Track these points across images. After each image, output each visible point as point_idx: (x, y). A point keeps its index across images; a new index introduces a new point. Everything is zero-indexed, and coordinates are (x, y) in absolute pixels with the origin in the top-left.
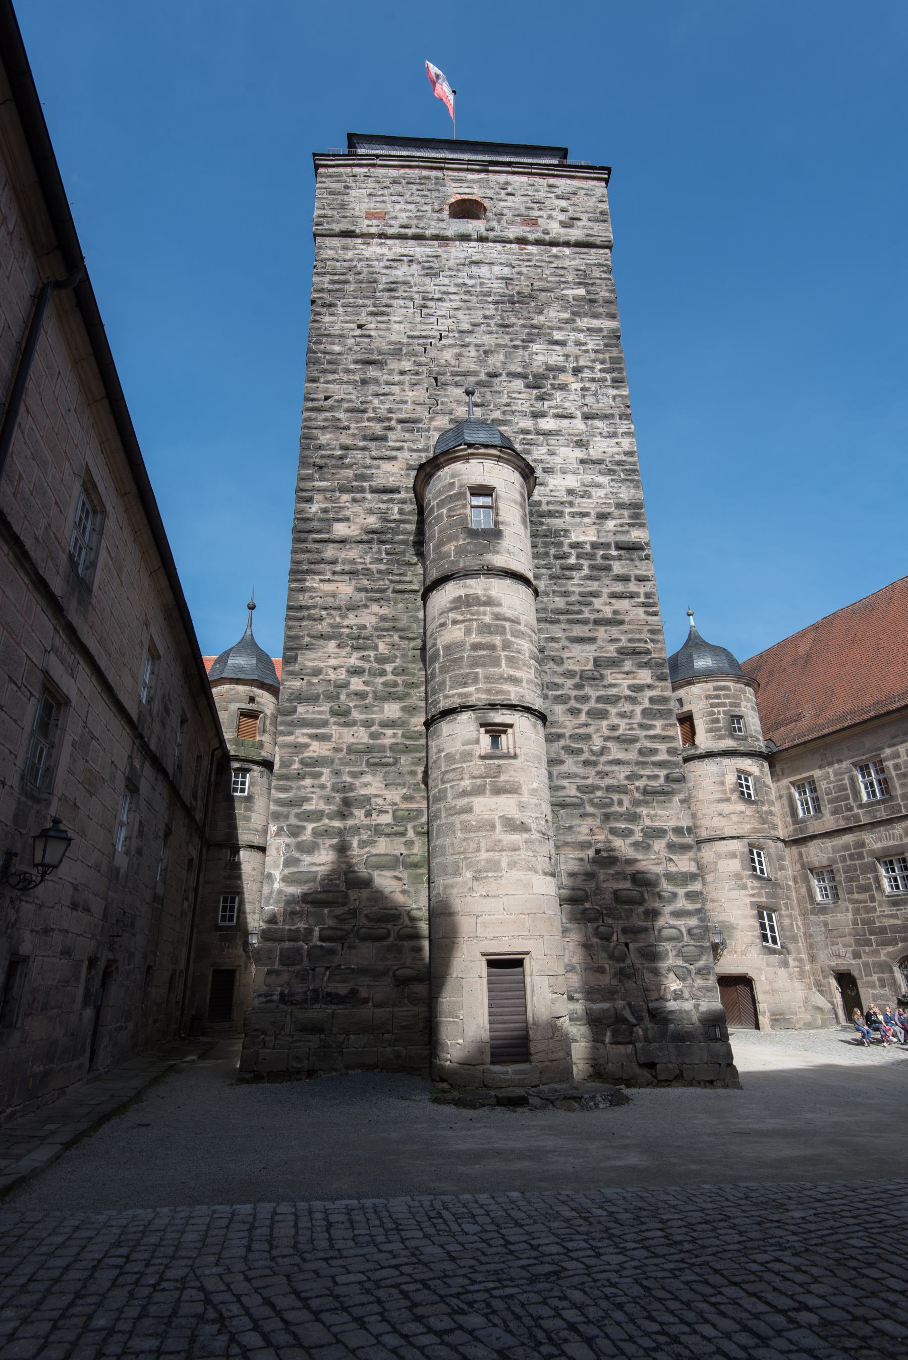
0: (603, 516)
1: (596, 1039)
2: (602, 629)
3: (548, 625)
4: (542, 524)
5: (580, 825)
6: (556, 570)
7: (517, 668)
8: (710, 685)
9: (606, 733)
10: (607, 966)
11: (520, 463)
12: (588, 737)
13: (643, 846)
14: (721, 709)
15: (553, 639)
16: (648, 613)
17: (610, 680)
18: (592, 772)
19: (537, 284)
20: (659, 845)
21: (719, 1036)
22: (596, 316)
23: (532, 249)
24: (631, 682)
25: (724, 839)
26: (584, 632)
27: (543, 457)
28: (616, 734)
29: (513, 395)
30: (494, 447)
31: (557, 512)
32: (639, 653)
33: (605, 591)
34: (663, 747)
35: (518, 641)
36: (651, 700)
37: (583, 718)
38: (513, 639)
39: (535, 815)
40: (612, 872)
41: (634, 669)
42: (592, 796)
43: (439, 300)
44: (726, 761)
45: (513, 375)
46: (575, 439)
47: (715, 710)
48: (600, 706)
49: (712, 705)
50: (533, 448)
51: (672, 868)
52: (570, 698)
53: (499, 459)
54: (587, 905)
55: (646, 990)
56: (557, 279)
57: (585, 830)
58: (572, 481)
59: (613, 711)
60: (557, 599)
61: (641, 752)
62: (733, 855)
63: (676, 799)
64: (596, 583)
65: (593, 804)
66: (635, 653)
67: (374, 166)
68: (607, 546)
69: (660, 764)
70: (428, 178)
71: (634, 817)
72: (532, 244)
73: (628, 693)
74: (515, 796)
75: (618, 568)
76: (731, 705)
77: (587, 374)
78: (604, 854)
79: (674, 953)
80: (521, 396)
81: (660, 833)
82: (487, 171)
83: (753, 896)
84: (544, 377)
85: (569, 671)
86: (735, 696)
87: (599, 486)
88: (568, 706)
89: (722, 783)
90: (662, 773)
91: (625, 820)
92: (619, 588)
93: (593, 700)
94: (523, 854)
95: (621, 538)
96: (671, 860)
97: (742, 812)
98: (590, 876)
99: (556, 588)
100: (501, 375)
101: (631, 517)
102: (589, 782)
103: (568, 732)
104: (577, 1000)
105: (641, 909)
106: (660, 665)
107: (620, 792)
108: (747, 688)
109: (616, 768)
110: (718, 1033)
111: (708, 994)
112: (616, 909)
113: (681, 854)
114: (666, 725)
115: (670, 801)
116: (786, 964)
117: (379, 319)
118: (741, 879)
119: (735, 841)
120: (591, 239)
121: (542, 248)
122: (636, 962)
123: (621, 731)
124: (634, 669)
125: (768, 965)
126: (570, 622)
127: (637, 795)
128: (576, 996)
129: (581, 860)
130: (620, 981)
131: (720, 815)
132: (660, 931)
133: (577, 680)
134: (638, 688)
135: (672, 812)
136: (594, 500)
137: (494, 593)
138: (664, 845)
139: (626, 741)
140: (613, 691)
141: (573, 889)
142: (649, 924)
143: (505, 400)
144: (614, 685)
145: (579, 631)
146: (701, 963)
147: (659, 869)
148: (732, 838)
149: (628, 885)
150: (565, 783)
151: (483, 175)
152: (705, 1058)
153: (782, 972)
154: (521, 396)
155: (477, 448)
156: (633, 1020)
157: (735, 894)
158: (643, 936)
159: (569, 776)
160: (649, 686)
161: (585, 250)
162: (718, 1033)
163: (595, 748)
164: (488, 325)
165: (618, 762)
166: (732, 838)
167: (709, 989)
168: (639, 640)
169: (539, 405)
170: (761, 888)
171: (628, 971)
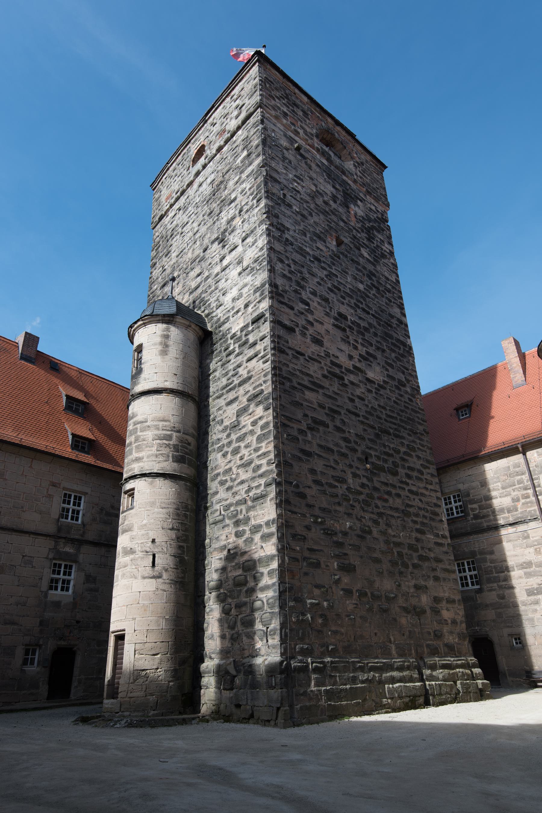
0: (246, 306)
1: (218, 687)
2: (241, 388)
3: (218, 400)
4: (220, 332)
5: (221, 535)
6: (224, 359)
7: (141, 451)
9: (239, 463)
10: (227, 634)
11: (158, 319)
12: (230, 469)
13: (250, 541)
15: (219, 409)
16: (264, 362)
17: (243, 423)
18: (230, 493)
19: (224, 171)
20: (257, 537)
21: (274, 685)
22: (250, 164)
23: (225, 149)
24: (252, 420)
26: (233, 395)
27: (223, 286)
28: (243, 461)
29: (212, 256)
30: (138, 320)
31: (226, 319)
32: (257, 395)
33: (245, 358)
34: (264, 461)
35: (144, 433)
36: (262, 428)
37: (229, 456)
38: (141, 434)
39: (140, 542)
40: (234, 564)
41: (255, 409)
42: (229, 511)
43: (187, 223)
45: (213, 242)
46: (237, 260)
48: (237, 445)
50: (220, 283)
51: (263, 554)
52: (224, 446)
53: (145, 324)
54: (222, 591)
55: (244, 650)
56: (233, 157)
57: (224, 537)
58: (234, 293)
59: (242, 444)
60: (224, 379)
61: (254, 471)
63: (269, 498)
64: (241, 356)
65: (229, 518)
66: (256, 396)
67: (168, 169)
68: (247, 326)
69: (261, 476)
70: (185, 153)
71: (247, 520)
72: (225, 145)
73: (251, 428)
74: (129, 533)
75: (251, 338)
77: (245, 208)
78: (232, 552)
79: (259, 619)
80: (216, 253)
81: (256, 529)
82: (207, 121)
84: (225, 230)
85: (225, 427)
87: (245, 285)
88: (223, 452)
90: (262, 481)
91: (243, 524)
92: (251, 352)
93: (234, 442)
94: (128, 569)
95: (255, 314)
96: (262, 547)
98: (224, 569)
99: (224, 372)
100: (208, 247)
101: (260, 296)
102: (228, 502)
103: (221, 470)
104: (213, 659)
105: (245, 589)
106: (267, 399)
107: (241, 504)
109: (240, 487)
110: (274, 682)
111: (274, 651)
112: (234, 591)
113: (269, 541)
114: (267, 444)
115: (266, 502)
117: (168, 256)
120: (249, 112)
121: (229, 143)
122: (240, 629)
123: (245, 459)
124: (255, 409)
126: (228, 392)
127: (250, 503)
128: (213, 656)
129: (221, 559)
130: (232, 644)
132: (253, 604)
133: (228, 431)
134: (254, 423)
135: (266, 510)
136: (245, 296)
137: (135, 410)
138: (259, 537)
139: (245, 465)
140: (244, 431)
141: (216, 581)
142: (248, 599)
143: (210, 261)
144: (244, 427)
145: (231, 396)
146: (272, 627)
147: (256, 556)
149: (240, 572)
150: (217, 507)
151: (205, 125)
152: (266, 702)
154: (216, 253)
155: (133, 326)
156: (234, 672)
158: (244, 609)
159: (220, 501)
160: (260, 418)
161: (248, 122)
162: (274, 682)
163: (234, 476)
164: (204, 220)
165: (242, 482)
167: (274, 647)
168: (258, 386)
169: (223, 252)
171: (235, 636)
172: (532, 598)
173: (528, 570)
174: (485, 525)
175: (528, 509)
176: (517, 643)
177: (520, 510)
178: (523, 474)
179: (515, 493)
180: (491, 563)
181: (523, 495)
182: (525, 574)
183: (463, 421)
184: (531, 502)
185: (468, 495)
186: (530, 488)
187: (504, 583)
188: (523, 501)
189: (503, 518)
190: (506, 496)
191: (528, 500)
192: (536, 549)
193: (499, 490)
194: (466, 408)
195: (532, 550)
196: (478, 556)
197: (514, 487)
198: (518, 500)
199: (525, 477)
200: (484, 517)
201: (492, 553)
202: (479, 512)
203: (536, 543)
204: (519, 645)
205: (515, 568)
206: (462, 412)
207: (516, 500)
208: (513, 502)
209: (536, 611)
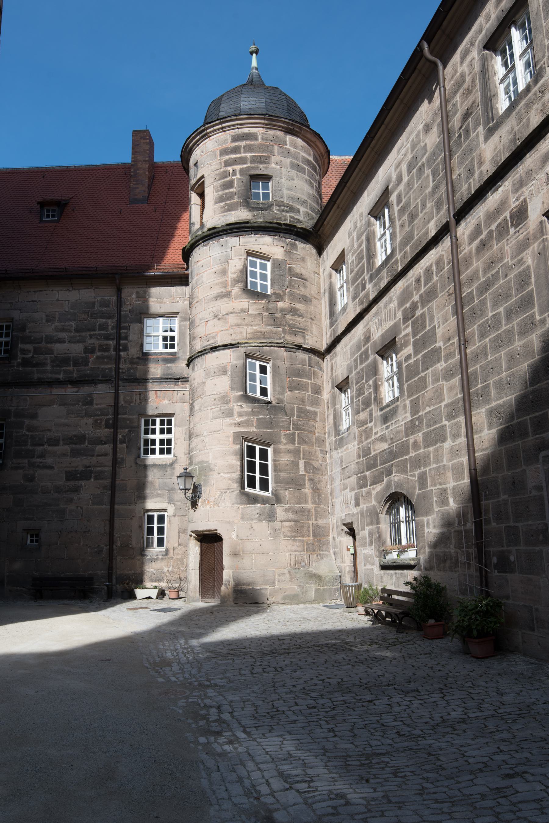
8: (228, 135)
14: (238, 167)
25: (214, 349)
44: (232, 241)
47: (230, 169)
49: (227, 163)
62: (223, 371)
76: (254, 160)
83: (239, 424)
86: (261, 148)
89: (224, 272)
97: (243, 311)
108: (289, 138)
116: (271, 517)
118: (228, 402)
119: (228, 352)
125: (243, 518)
131: (216, 316)
148: (226, 346)
153: (264, 527)
157: (218, 424)
166: (226, 346)
170: (253, 413)
172: (71, 483)
173: (78, 446)
174: (36, 376)
175: (102, 367)
176: (32, 541)
177: (90, 366)
178: (109, 317)
179: (92, 341)
180: (28, 430)
181: (101, 346)
182: (72, 450)
183: (47, 225)
184: (109, 358)
185: (23, 329)
186: (113, 339)
187: (39, 460)
188: (99, 354)
189: (65, 371)
190: (78, 342)
191: (106, 354)
192: (96, 421)
193: (70, 331)
194: (56, 208)
195: (91, 420)
196: (13, 419)
197: (92, 333)
198: (93, 351)
199: (111, 323)
200: (37, 365)
201: (34, 416)
202: (33, 357)
203: (99, 413)
204: (35, 544)
205: (61, 442)
206: (48, 211)
207: (90, 350)
208: (85, 353)
209: (71, 500)
